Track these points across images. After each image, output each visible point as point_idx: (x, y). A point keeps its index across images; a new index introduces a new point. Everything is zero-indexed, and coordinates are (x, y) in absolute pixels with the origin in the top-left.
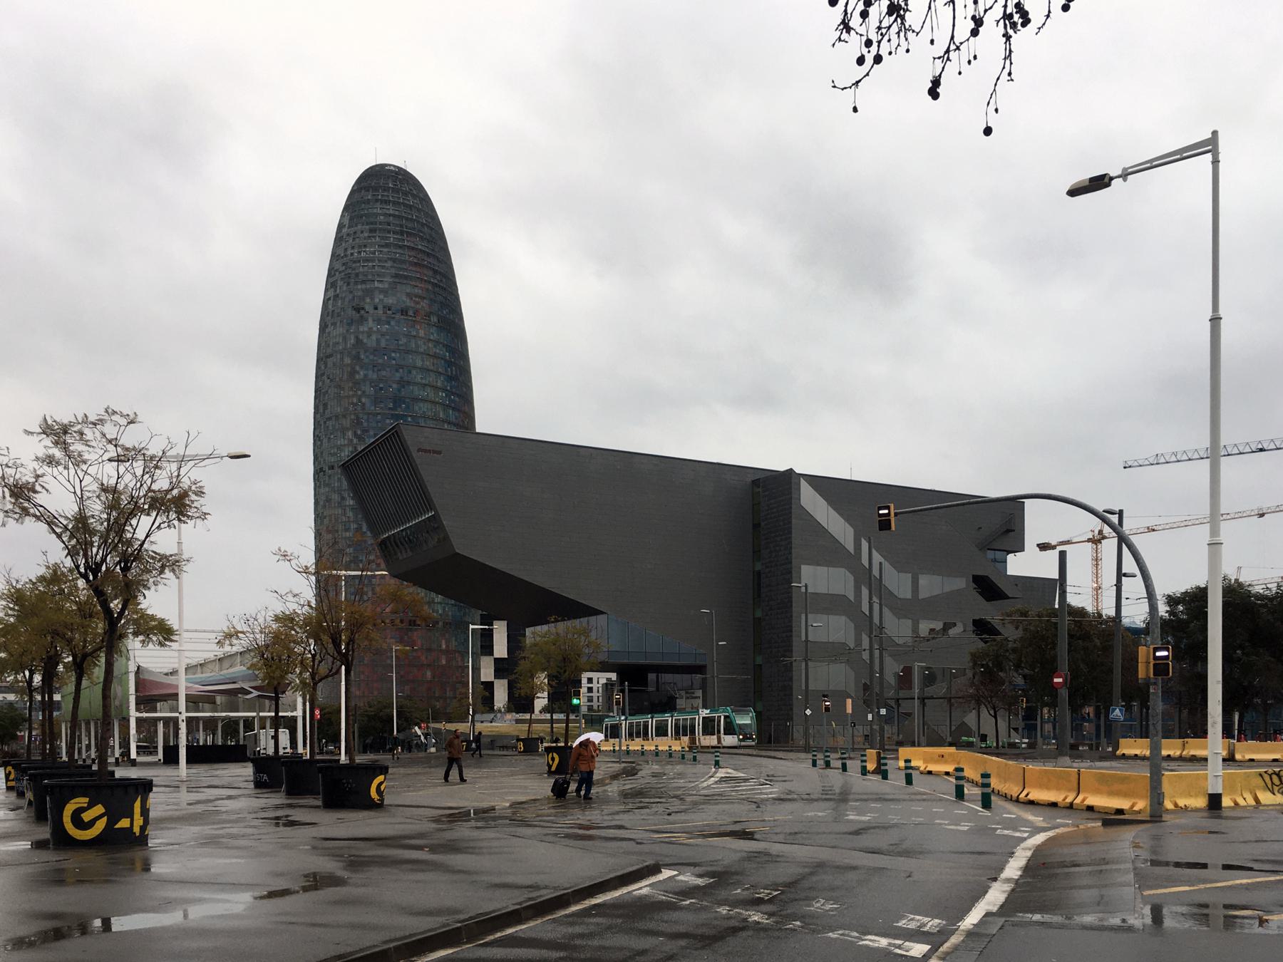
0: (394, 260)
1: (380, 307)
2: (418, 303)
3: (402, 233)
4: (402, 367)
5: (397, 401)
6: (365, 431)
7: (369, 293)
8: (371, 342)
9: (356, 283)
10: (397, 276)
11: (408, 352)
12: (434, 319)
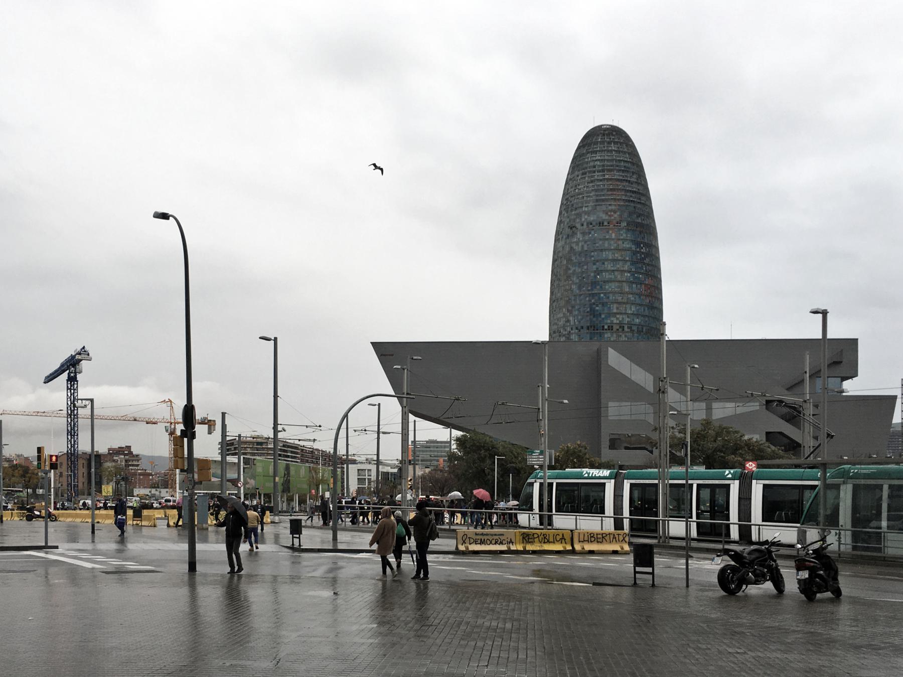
0: (596, 190)
1: (585, 224)
2: (610, 216)
3: (603, 171)
4: (597, 261)
5: (594, 284)
6: (573, 307)
7: (579, 215)
8: (578, 248)
9: (572, 211)
10: (597, 201)
11: (602, 250)
12: (624, 224)
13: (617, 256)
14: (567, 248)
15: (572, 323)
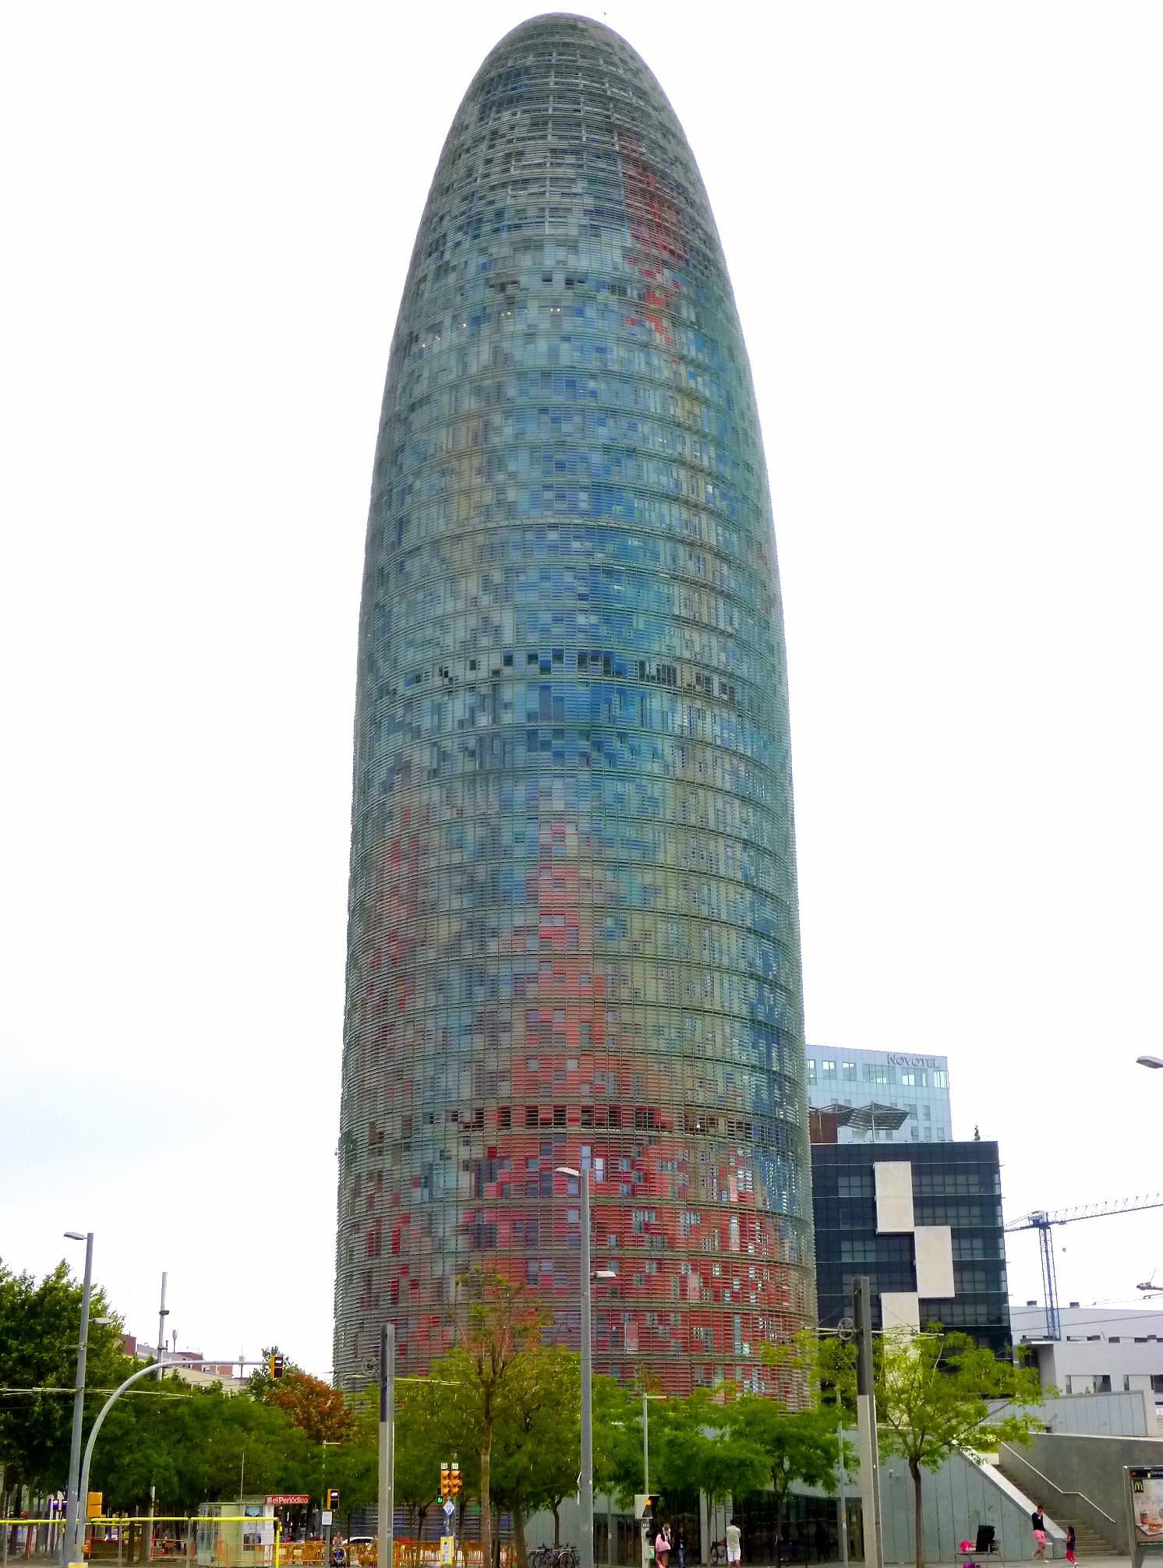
13: (678, 411)
14: (483, 355)
15: (508, 637)
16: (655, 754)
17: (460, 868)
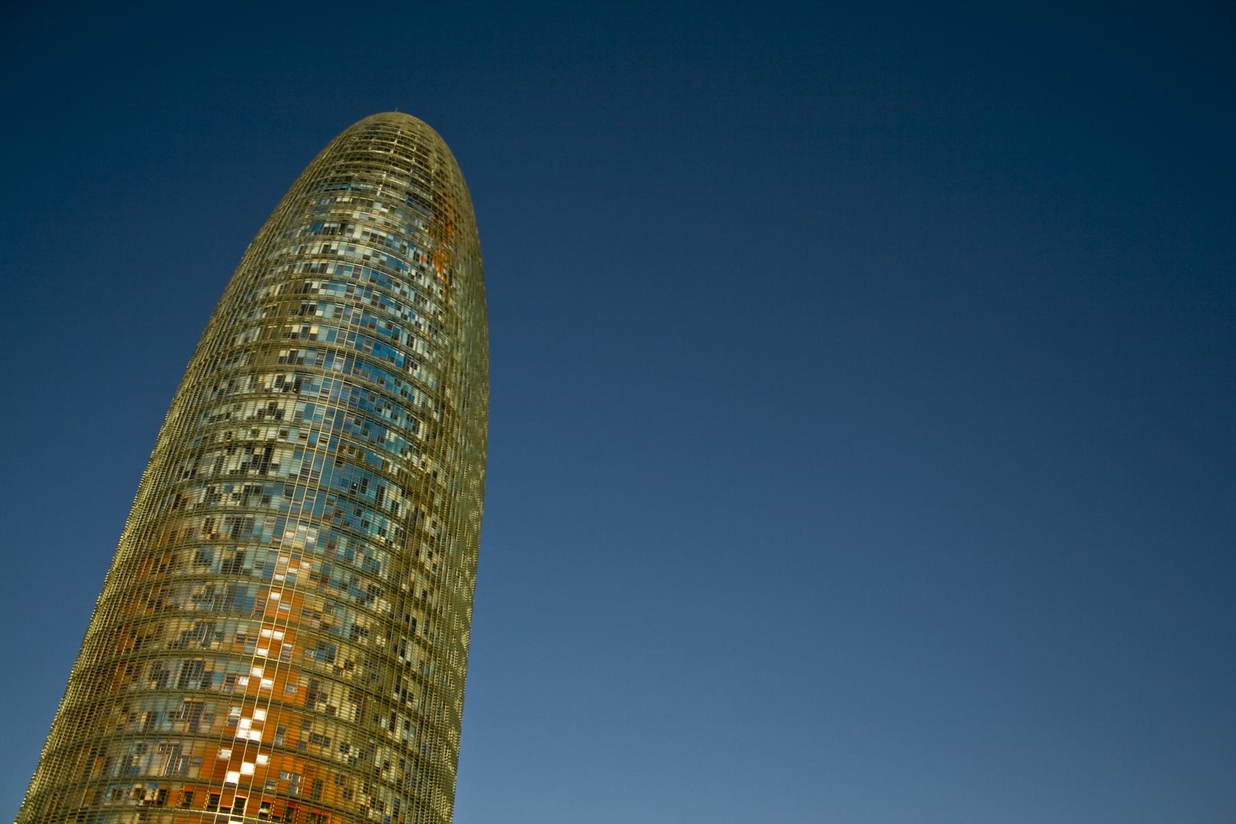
16: (382, 532)
17: (203, 579)
